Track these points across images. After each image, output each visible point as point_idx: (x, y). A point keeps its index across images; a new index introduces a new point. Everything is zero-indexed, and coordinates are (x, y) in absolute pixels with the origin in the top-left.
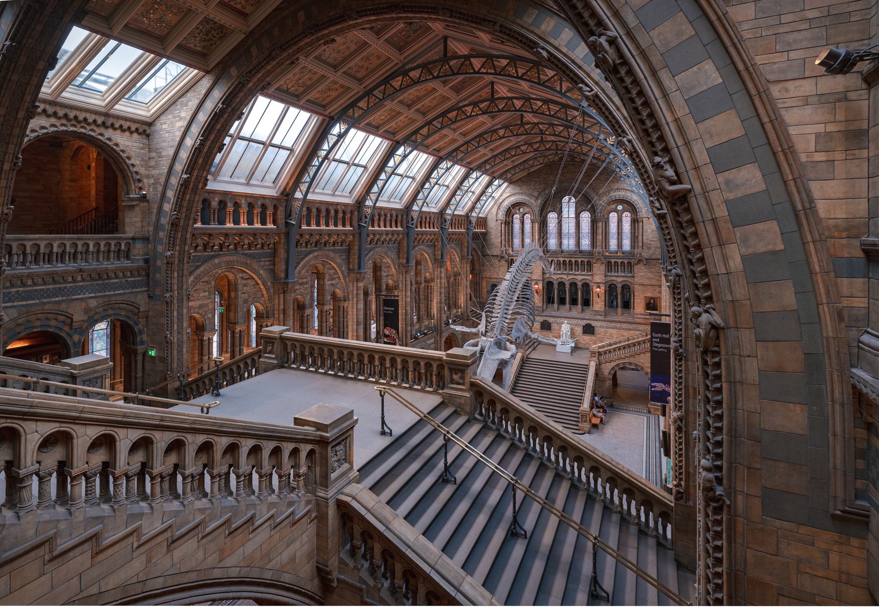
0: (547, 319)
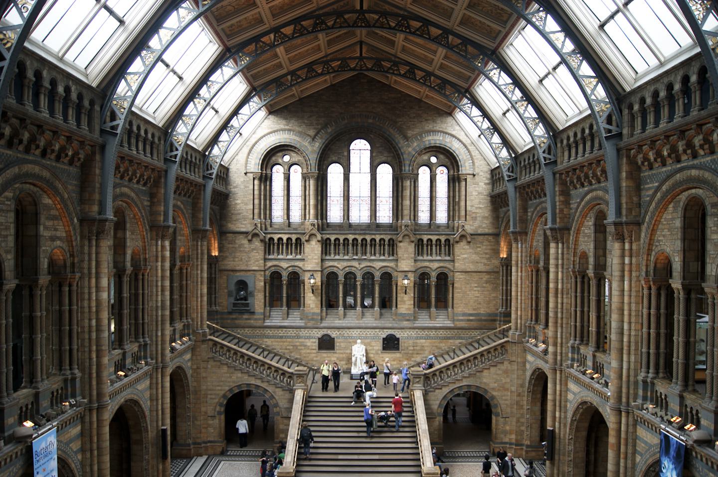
0: (329, 332)
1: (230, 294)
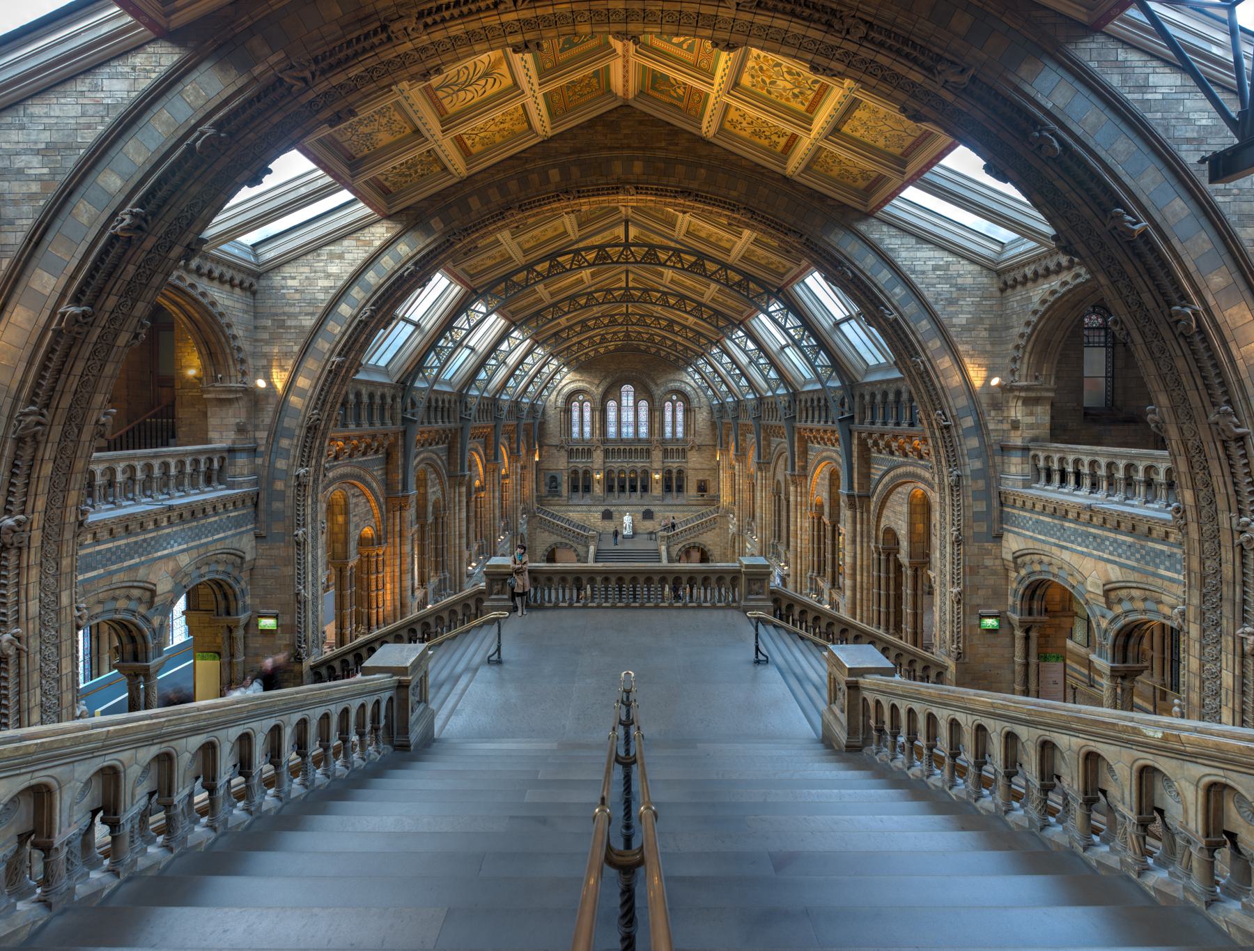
1: (546, 485)
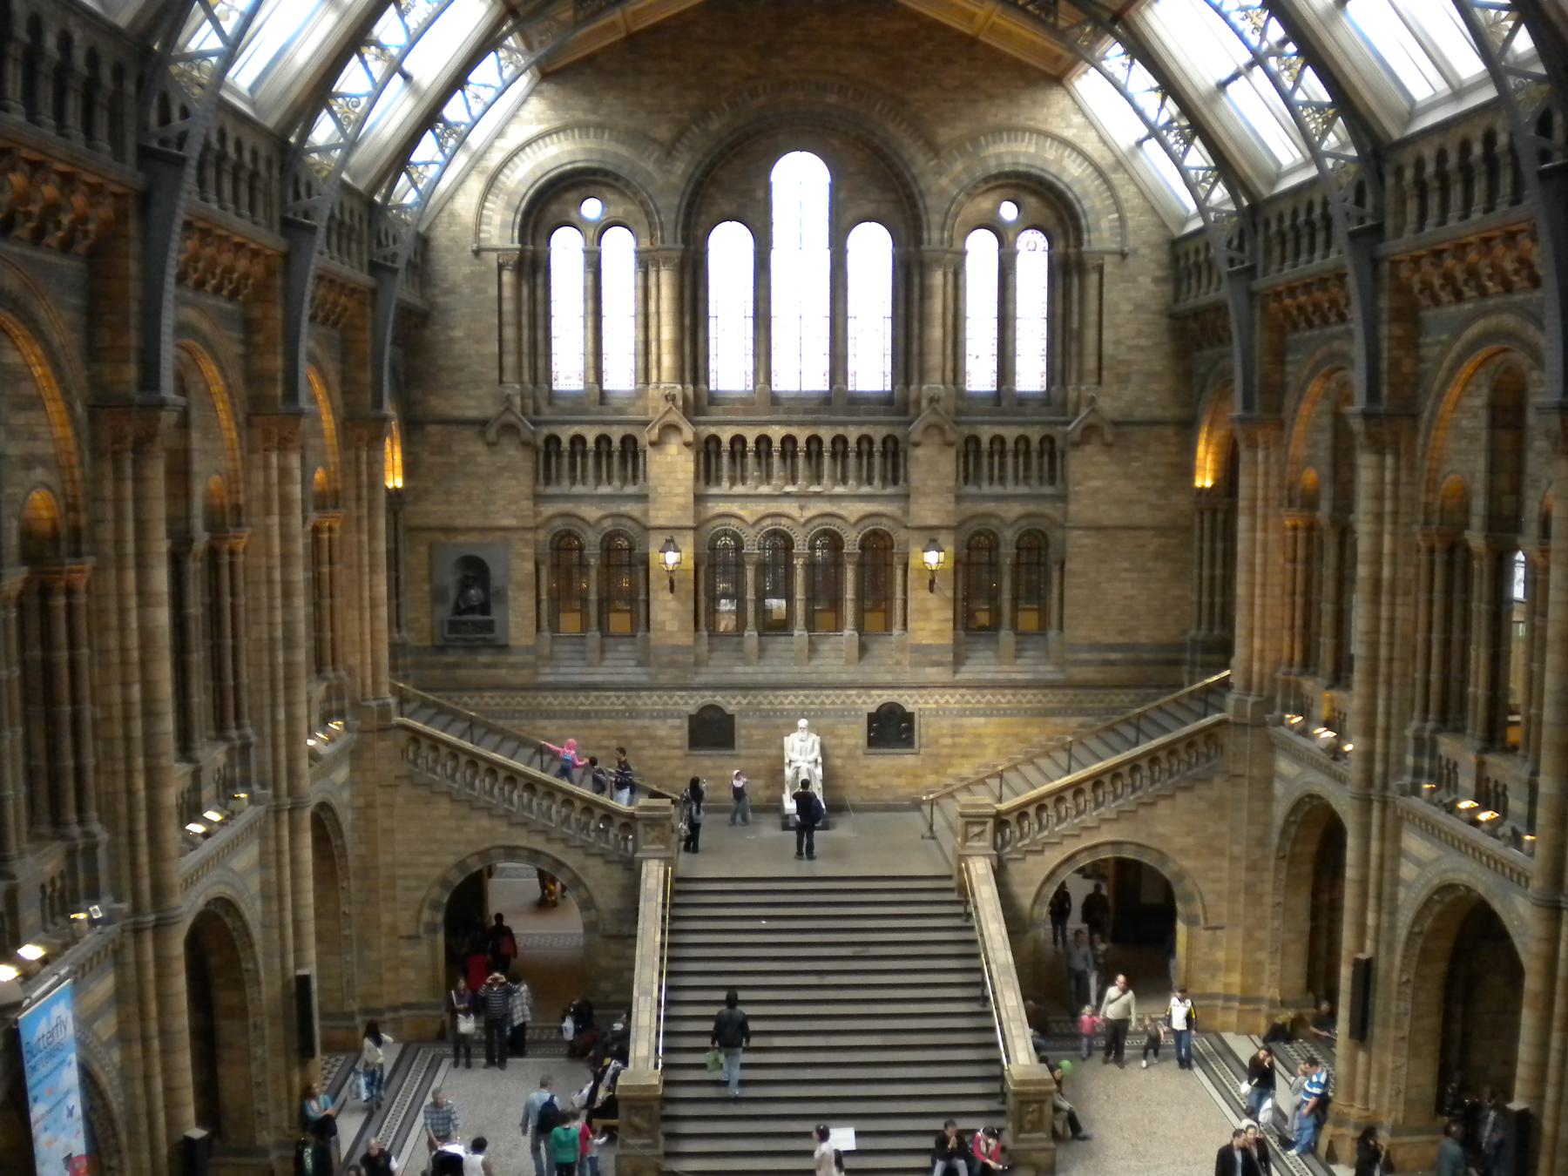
0: (719, 699)
1: (437, 597)
